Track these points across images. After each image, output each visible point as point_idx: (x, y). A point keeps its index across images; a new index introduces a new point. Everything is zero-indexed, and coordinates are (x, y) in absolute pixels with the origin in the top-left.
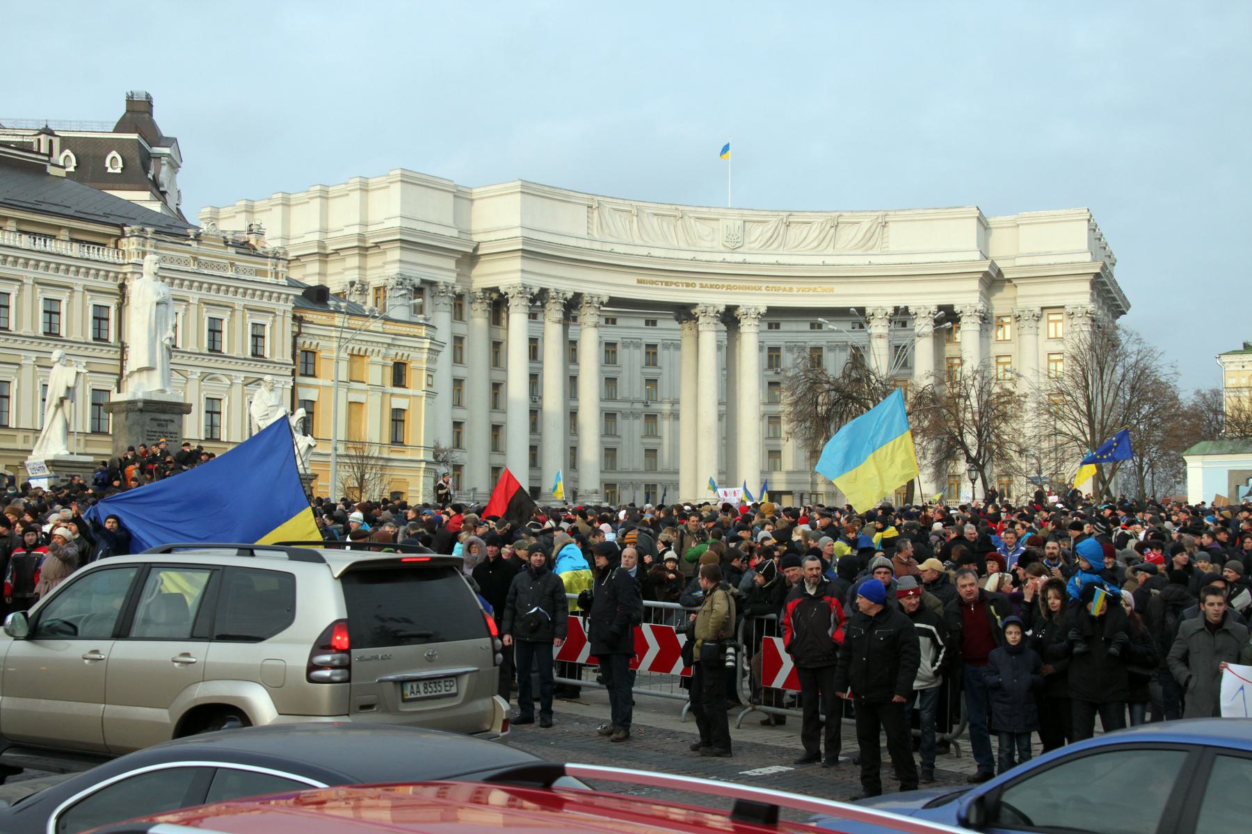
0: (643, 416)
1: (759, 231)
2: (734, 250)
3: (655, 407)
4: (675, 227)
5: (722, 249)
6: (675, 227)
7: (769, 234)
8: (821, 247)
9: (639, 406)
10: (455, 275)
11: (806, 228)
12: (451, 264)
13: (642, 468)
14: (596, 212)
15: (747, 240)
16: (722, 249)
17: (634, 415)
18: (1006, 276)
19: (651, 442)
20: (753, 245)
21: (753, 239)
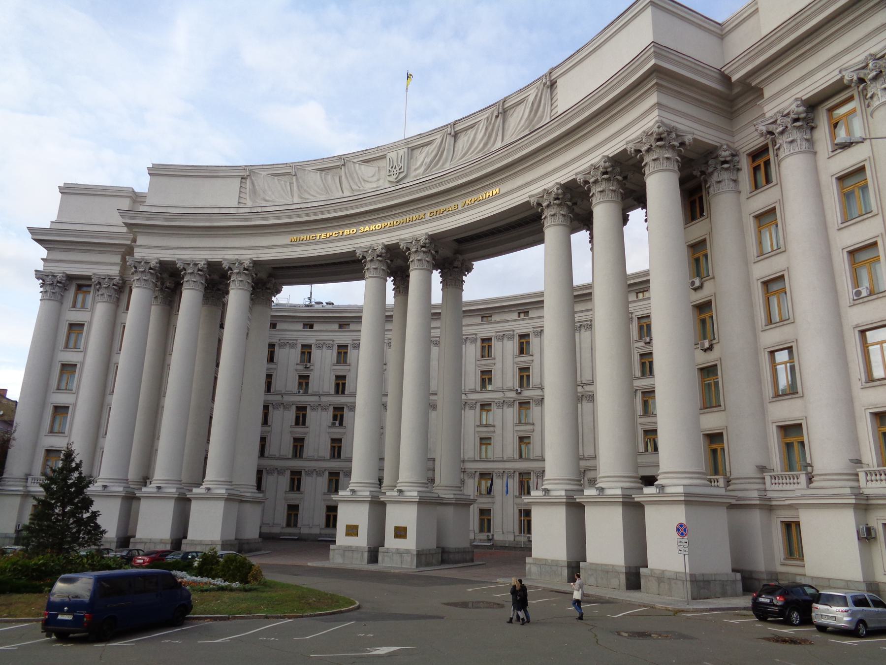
0: (516, 404)
1: (423, 155)
2: (398, 182)
3: (527, 393)
4: (340, 178)
5: (387, 185)
6: (340, 178)
7: (434, 153)
8: (490, 145)
9: (513, 394)
10: (118, 268)
11: (471, 133)
12: (117, 259)
13: (517, 456)
14: (248, 181)
15: (413, 168)
16: (387, 185)
17: (511, 404)
18: (734, 78)
19: (524, 429)
20: (418, 172)
21: (419, 163)
